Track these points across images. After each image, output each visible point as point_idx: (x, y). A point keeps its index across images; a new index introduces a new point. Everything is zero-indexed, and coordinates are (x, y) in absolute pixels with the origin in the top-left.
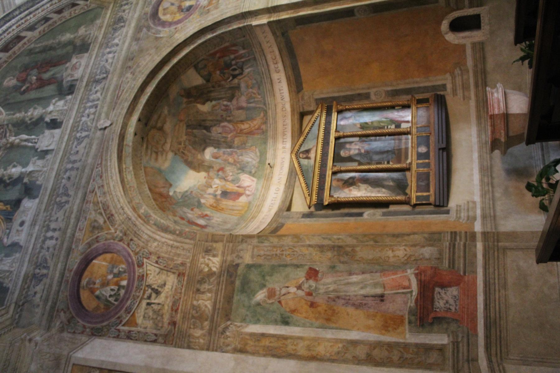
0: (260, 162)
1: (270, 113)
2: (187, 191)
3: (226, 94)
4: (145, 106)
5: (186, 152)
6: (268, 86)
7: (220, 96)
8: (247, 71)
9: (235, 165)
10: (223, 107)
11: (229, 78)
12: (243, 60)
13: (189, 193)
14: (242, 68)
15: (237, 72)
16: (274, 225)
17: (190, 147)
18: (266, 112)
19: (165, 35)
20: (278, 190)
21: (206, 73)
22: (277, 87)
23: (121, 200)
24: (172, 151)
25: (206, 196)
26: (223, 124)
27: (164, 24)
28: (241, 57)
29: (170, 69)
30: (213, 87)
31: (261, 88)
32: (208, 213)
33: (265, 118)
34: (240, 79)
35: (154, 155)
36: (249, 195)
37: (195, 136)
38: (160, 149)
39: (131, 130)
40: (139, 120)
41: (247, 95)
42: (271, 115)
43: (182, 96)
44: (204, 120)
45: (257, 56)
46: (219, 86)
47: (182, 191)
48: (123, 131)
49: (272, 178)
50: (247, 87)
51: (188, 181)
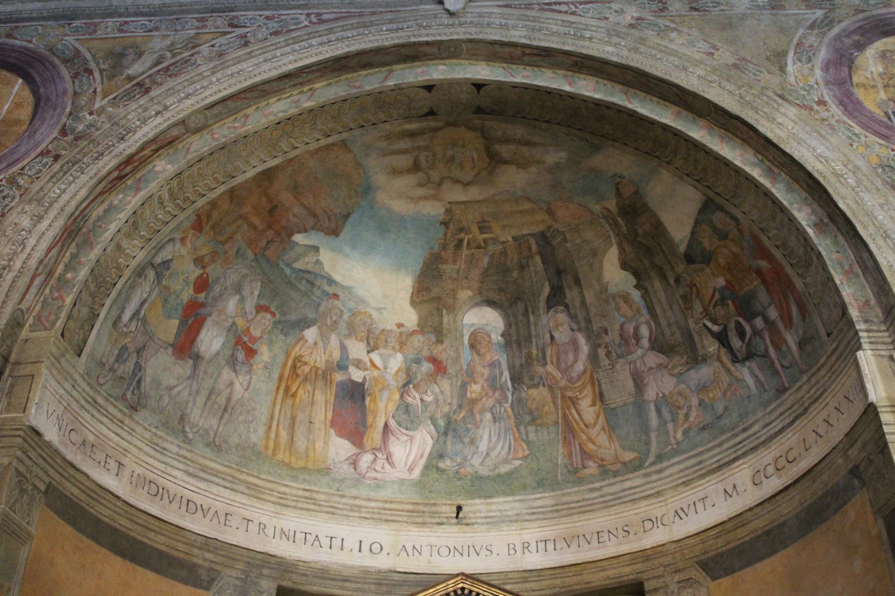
0: (478, 478)
1: (636, 480)
2: (331, 281)
3: (669, 325)
4: (527, 88)
5: (465, 252)
6: (712, 458)
7: (658, 311)
8: (745, 373)
9: (460, 407)
10: (630, 328)
11: (715, 322)
12: (772, 352)
13: (330, 290)
14: (749, 356)
15: (736, 343)
16: (199, 558)
17: (486, 260)
18: (635, 467)
19: (792, 79)
20: (376, 549)
21: (706, 243)
22: (711, 486)
23: (188, 102)
24: (448, 211)
25: (334, 340)
26: (582, 340)
27: (842, 63)
28: (779, 343)
29: (665, 128)
30: (677, 281)
31: (705, 435)
32: (264, 354)
33: (619, 466)
34: (719, 359)
35: (405, 161)
36: (354, 463)
37: (522, 268)
38: (435, 176)
39: (438, 72)
40: (479, 86)
41: (680, 394)
42: (628, 484)
43: (618, 193)
44: (578, 282)
45: (789, 399)
46: (685, 297)
47: (327, 268)
48: (428, 49)
49: (423, 524)
50: (703, 388)
51: (374, 281)
